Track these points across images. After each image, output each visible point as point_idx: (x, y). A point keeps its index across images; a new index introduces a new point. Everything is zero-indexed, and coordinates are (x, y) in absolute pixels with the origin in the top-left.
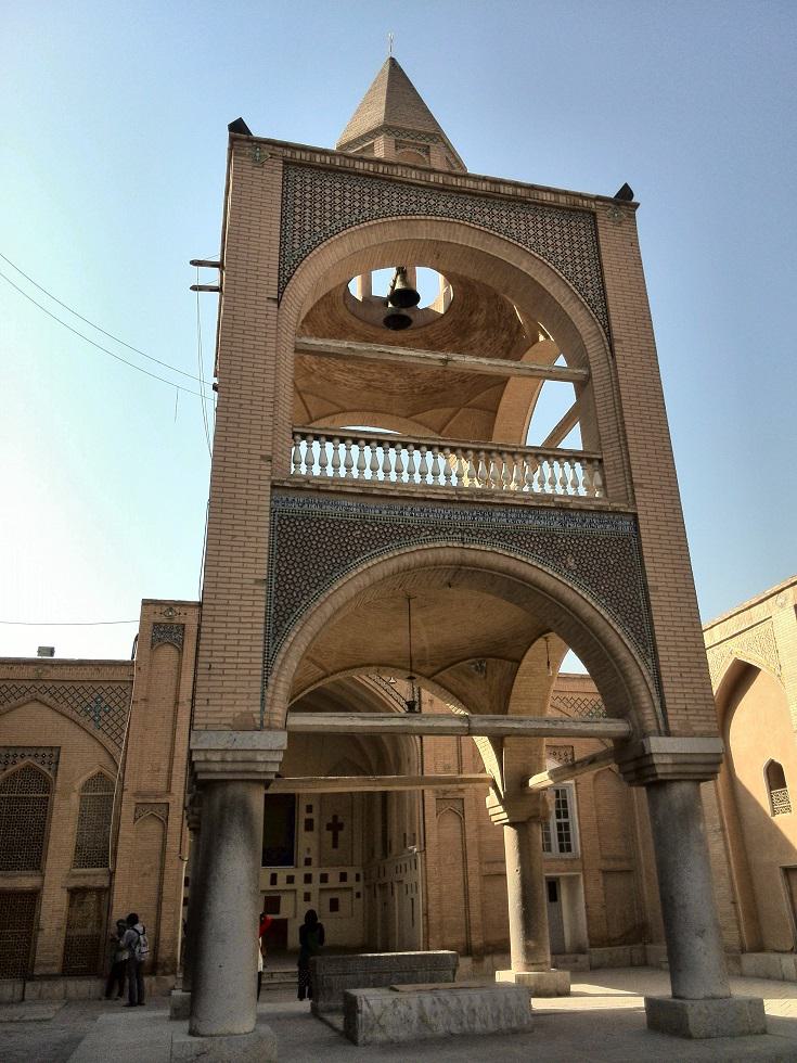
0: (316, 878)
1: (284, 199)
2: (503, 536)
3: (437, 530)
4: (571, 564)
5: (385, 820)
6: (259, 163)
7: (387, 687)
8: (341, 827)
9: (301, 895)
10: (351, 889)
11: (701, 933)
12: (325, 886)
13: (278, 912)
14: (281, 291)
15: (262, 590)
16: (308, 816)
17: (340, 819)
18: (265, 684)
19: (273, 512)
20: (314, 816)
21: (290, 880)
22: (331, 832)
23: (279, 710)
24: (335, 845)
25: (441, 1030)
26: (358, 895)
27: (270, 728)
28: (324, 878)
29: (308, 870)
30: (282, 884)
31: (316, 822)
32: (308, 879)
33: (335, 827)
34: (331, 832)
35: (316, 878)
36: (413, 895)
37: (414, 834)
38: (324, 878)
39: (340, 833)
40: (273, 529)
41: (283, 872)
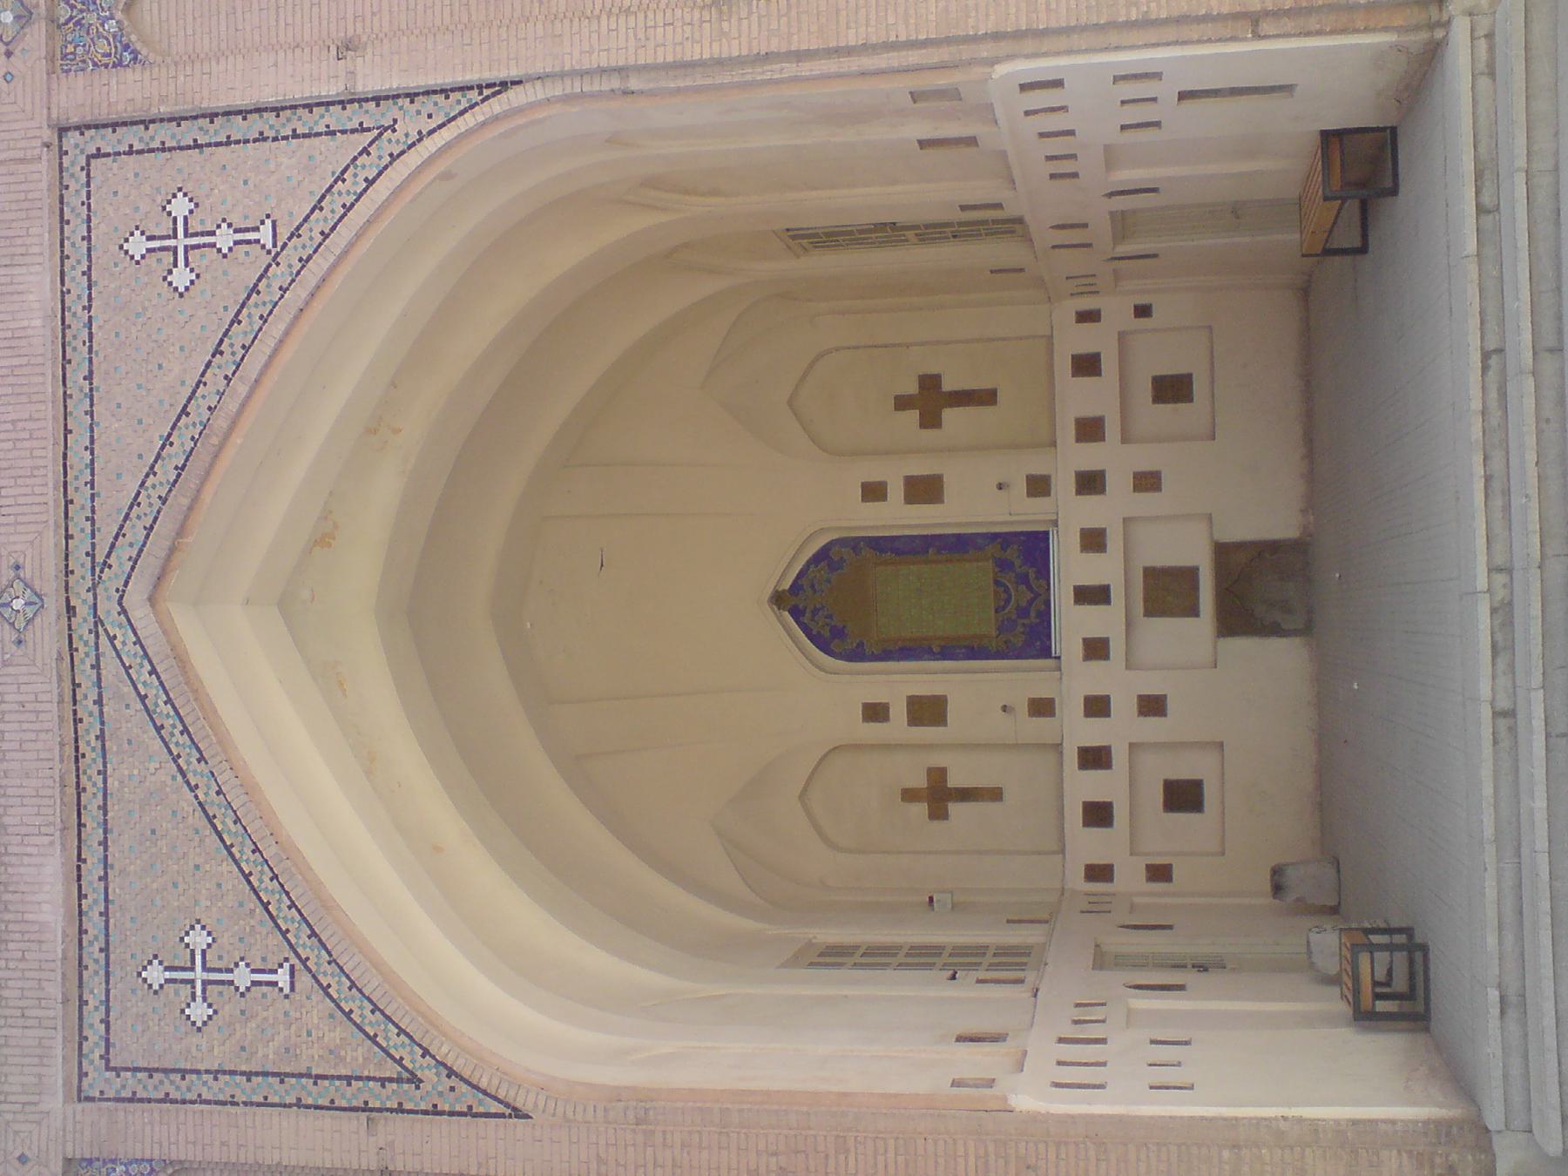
0: (1090, 457)
5: (888, 232)
7: (291, 256)
8: (930, 383)
9: (1146, 503)
10: (1122, 337)
12: (1112, 429)
13: (1191, 574)
16: (896, 491)
17: (912, 388)
20: (894, 475)
21: (1093, 540)
22: (948, 414)
24: (987, 398)
26: (1143, 311)
28: (1090, 430)
29: (1064, 484)
30: (1103, 569)
31: (920, 467)
32: (1090, 483)
33: (931, 400)
34: (948, 414)
35: (1090, 457)
36: (1166, 91)
37: (915, 96)
38: (1090, 430)
39: (948, 385)
41: (1069, 567)
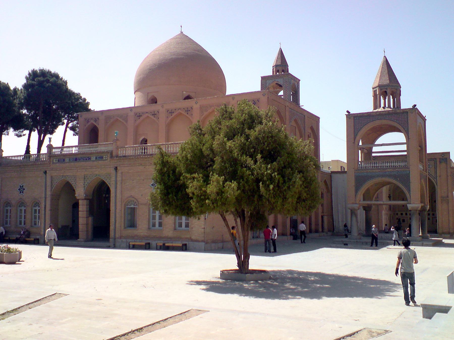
6: (350, 118)
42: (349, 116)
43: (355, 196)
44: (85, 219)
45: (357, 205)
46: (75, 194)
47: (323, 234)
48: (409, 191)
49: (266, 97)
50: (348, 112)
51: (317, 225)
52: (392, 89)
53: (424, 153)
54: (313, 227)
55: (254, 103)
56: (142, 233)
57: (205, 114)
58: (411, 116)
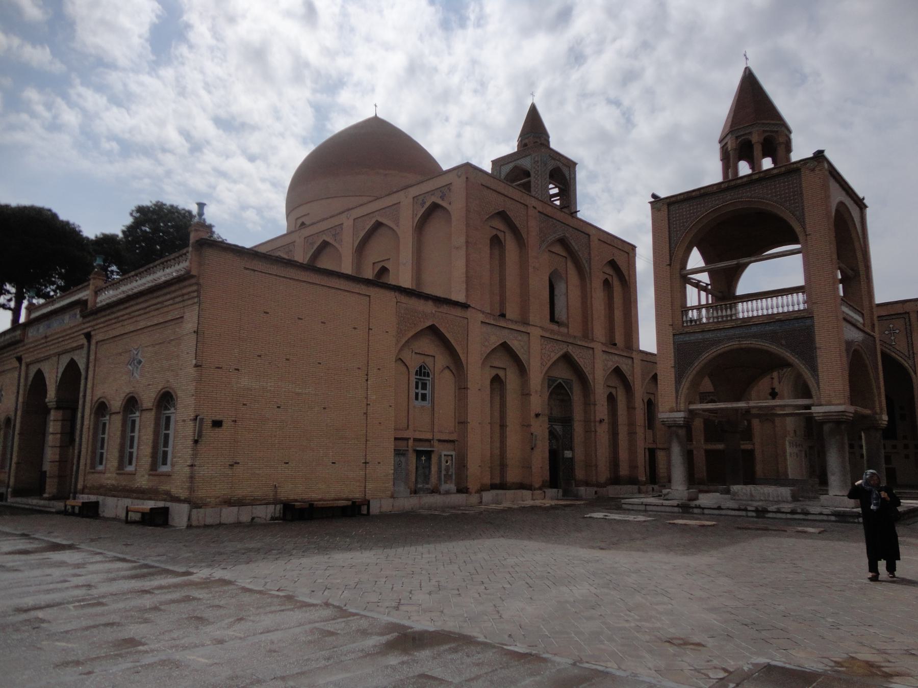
1: (669, 220)
2: (754, 336)
3: (730, 339)
4: (783, 342)
6: (659, 210)
11: (833, 474)
14: (671, 260)
15: (673, 370)
18: (677, 398)
19: (674, 343)
21: (894, 447)
23: (682, 407)
25: (757, 498)
27: (680, 411)
32: (906, 447)
40: (674, 348)
42: (657, 202)
43: (677, 391)
44: (57, 450)
45: (682, 415)
46: (46, 397)
47: (650, 487)
48: (814, 369)
49: (464, 178)
50: (654, 196)
51: (633, 467)
52: (764, 131)
53: (775, 171)
54: (624, 471)
55: (442, 198)
56: (108, 479)
57: (362, 234)
58: (809, 180)
